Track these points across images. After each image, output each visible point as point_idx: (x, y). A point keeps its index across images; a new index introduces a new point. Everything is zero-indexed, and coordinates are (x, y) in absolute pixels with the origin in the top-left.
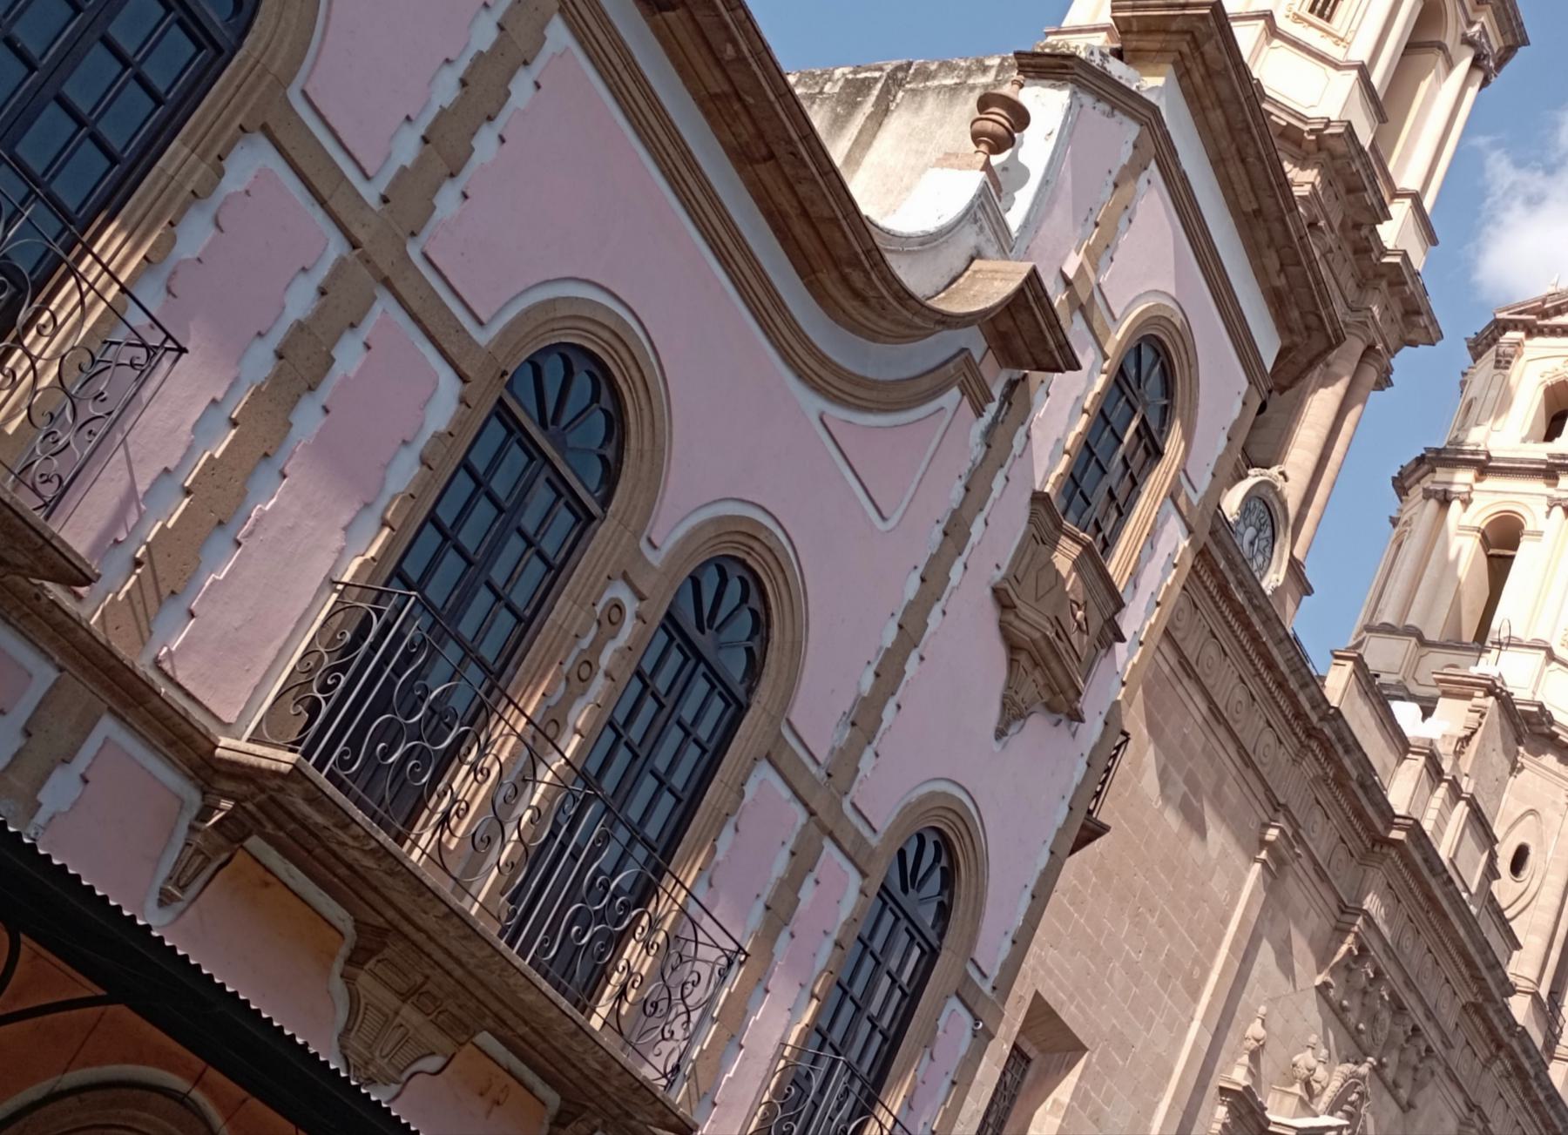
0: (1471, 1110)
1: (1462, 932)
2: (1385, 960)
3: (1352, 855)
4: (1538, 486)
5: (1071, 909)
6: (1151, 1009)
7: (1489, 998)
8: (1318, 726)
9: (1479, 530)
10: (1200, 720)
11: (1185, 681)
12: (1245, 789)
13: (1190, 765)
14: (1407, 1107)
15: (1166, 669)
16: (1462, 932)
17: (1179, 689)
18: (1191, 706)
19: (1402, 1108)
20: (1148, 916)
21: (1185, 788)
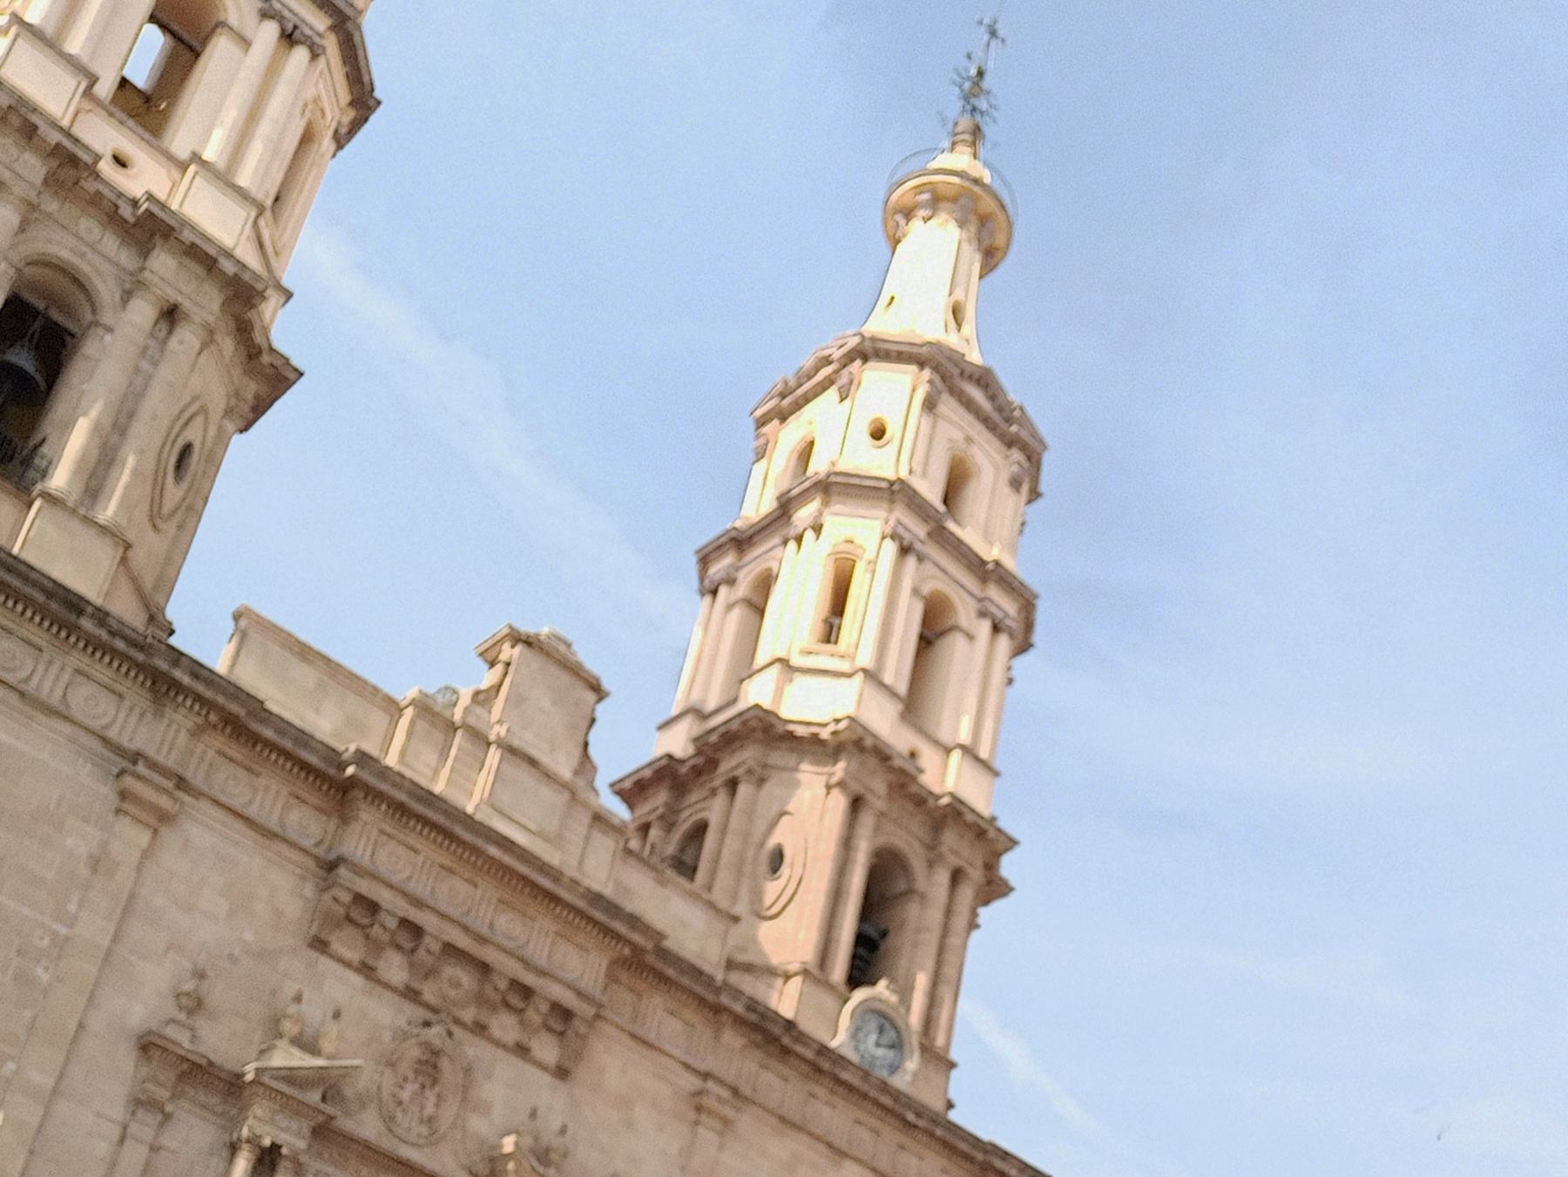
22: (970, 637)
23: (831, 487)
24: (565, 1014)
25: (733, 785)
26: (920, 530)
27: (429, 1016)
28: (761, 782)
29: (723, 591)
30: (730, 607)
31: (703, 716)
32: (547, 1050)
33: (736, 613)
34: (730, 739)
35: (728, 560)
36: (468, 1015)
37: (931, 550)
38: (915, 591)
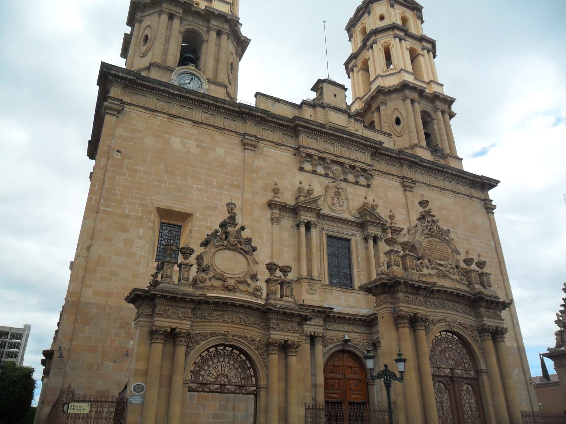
0: (403, 179)
1: (345, 136)
2: (321, 154)
3: (293, 137)
4: (365, 50)
5: (160, 184)
6: (218, 197)
7: (377, 149)
8: (240, 110)
9: (361, 69)
10: (191, 126)
11: (176, 119)
12: (226, 135)
13: (194, 137)
14: (368, 186)
15: (166, 119)
16: (345, 136)
17: (175, 122)
18: (183, 124)
19: (367, 187)
20: (200, 176)
21: (197, 143)
22: (423, 56)
23: (376, 32)
24: (364, 170)
25: (378, 109)
26: (402, 34)
27: (334, 180)
28: (386, 104)
29: (354, 69)
30: (358, 72)
31: (360, 99)
32: (362, 180)
33: (360, 73)
34: (373, 98)
35: (354, 61)
36: (342, 178)
37: (405, 37)
38: (406, 48)
